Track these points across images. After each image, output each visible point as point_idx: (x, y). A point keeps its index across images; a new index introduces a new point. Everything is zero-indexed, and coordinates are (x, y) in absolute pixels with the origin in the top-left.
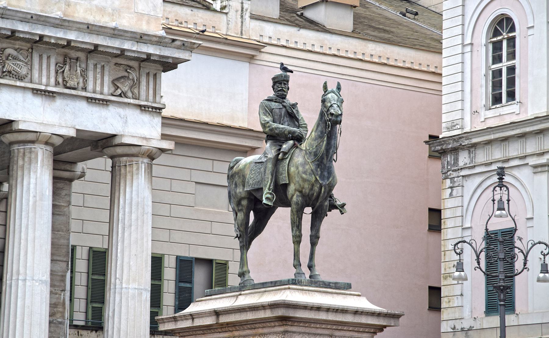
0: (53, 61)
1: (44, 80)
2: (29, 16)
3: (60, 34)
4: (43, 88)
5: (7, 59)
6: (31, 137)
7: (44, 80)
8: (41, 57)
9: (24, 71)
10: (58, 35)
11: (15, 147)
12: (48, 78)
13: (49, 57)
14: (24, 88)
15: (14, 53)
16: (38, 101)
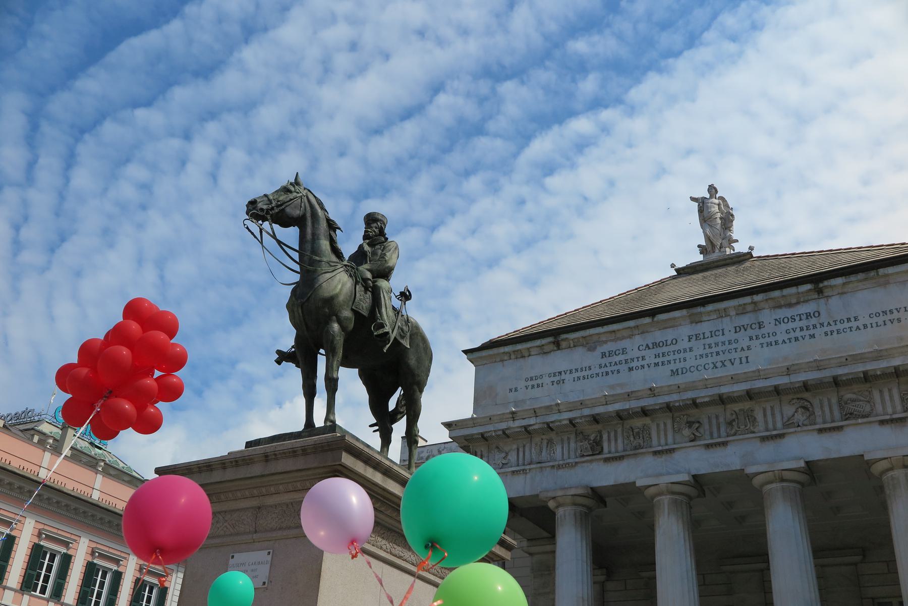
0: (895, 392)
1: (890, 410)
2: (844, 360)
3: (883, 364)
4: (888, 417)
5: (846, 403)
6: (884, 465)
7: (890, 410)
8: (881, 391)
9: (868, 408)
10: (882, 366)
11: (884, 477)
12: (894, 407)
13: (890, 390)
14: (870, 422)
15: (854, 396)
16: (886, 430)
